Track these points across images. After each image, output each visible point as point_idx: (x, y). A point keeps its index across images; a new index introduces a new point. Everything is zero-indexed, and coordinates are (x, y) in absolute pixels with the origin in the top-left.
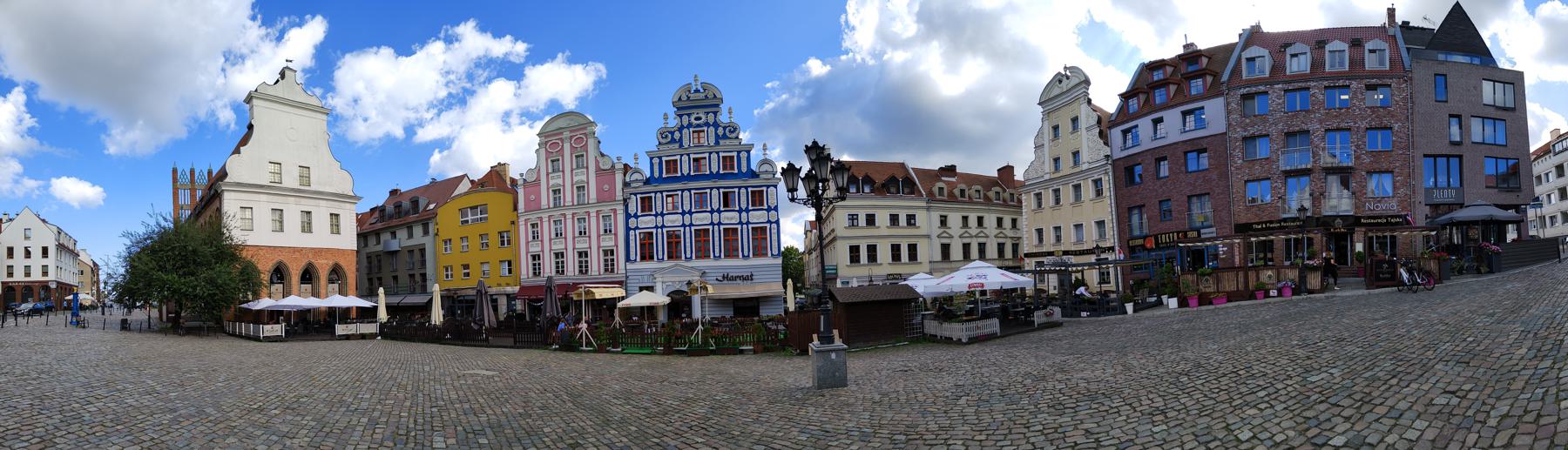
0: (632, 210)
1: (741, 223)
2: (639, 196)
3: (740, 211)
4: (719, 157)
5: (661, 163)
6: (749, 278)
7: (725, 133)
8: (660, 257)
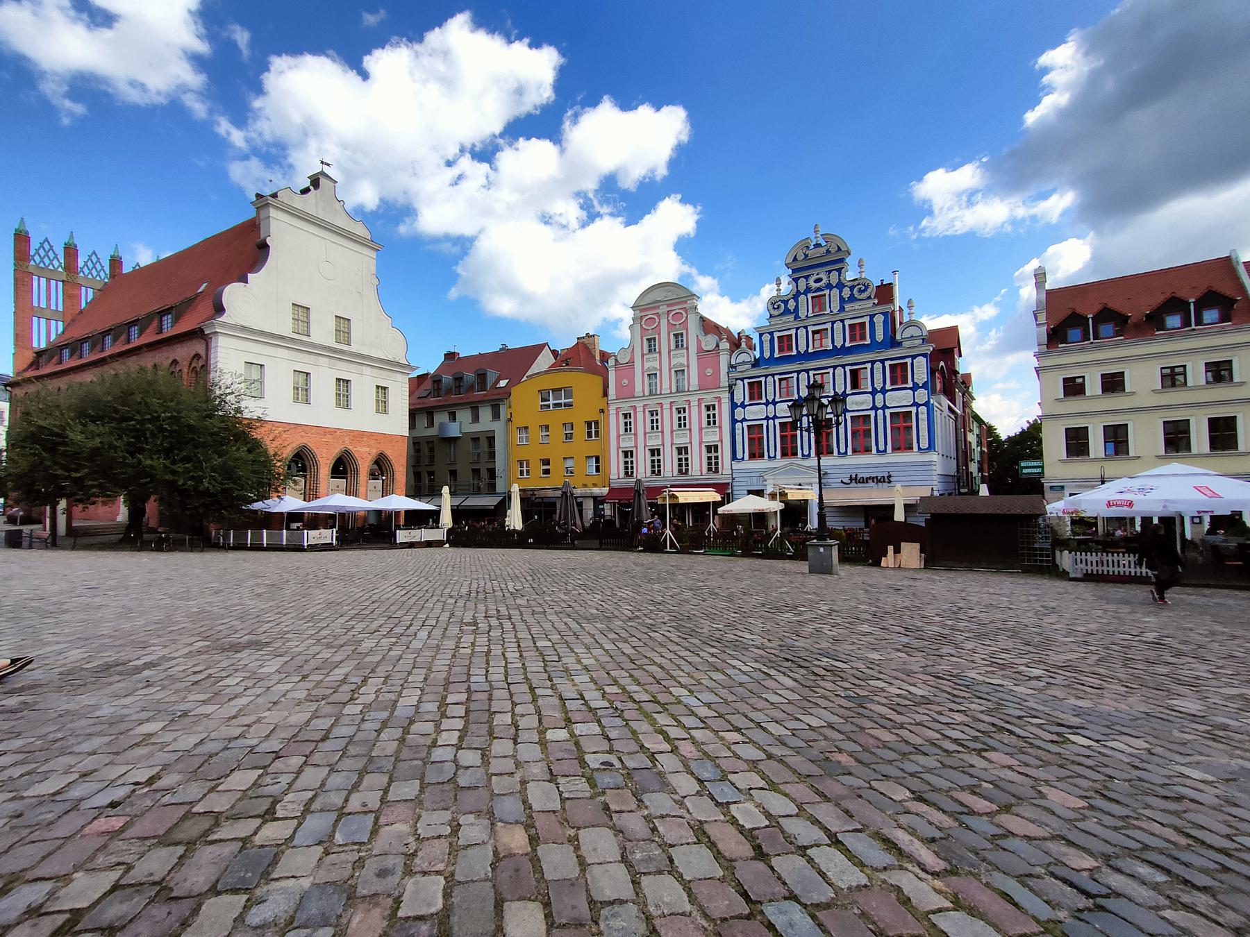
0: (738, 398)
1: (874, 408)
2: (746, 381)
3: (874, 392)
5: (772, 341)
6: (887, 480)
7: (852, 294)
8: (772, 454)
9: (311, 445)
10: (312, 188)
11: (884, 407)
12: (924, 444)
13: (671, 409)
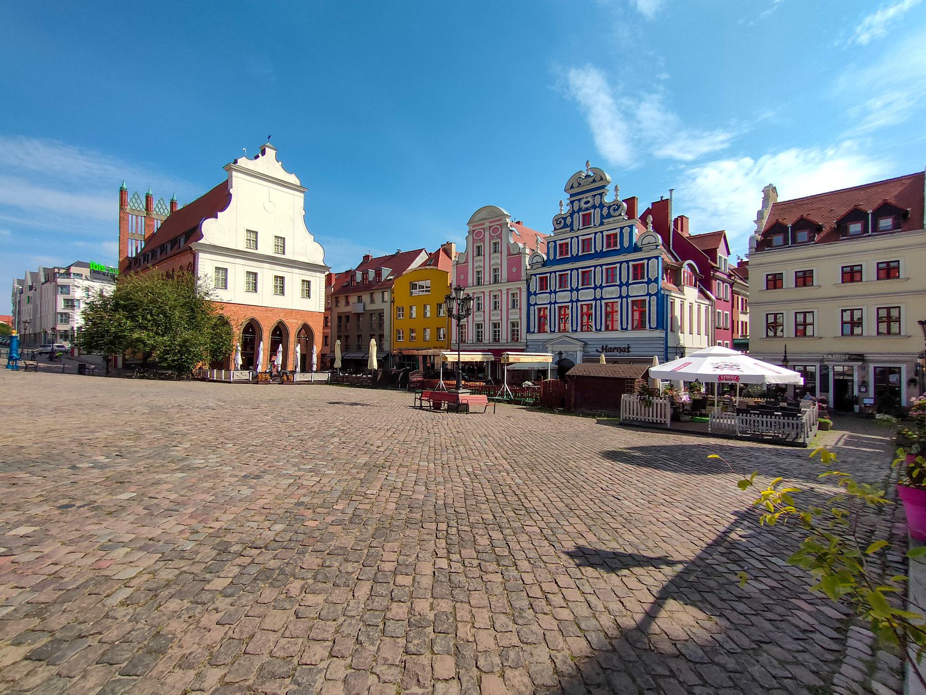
0: (532, 290)
1: (621, 297)
3: (621, 286)
4: (603, 236)
7: (609, 212)
9: (257, 318)
10: (260, 155)
11: (628, 296)
12: (654, 325)
13: (490, 295)
